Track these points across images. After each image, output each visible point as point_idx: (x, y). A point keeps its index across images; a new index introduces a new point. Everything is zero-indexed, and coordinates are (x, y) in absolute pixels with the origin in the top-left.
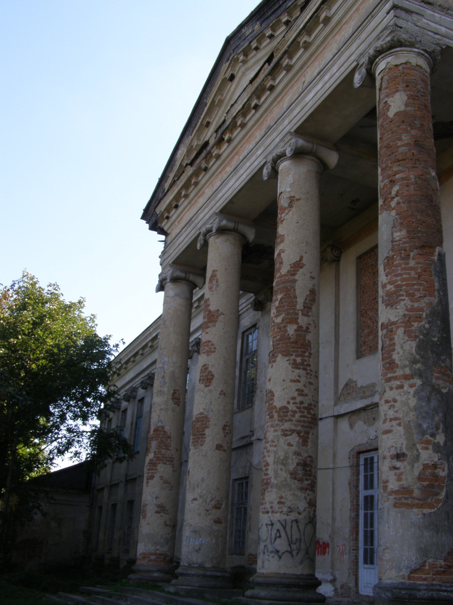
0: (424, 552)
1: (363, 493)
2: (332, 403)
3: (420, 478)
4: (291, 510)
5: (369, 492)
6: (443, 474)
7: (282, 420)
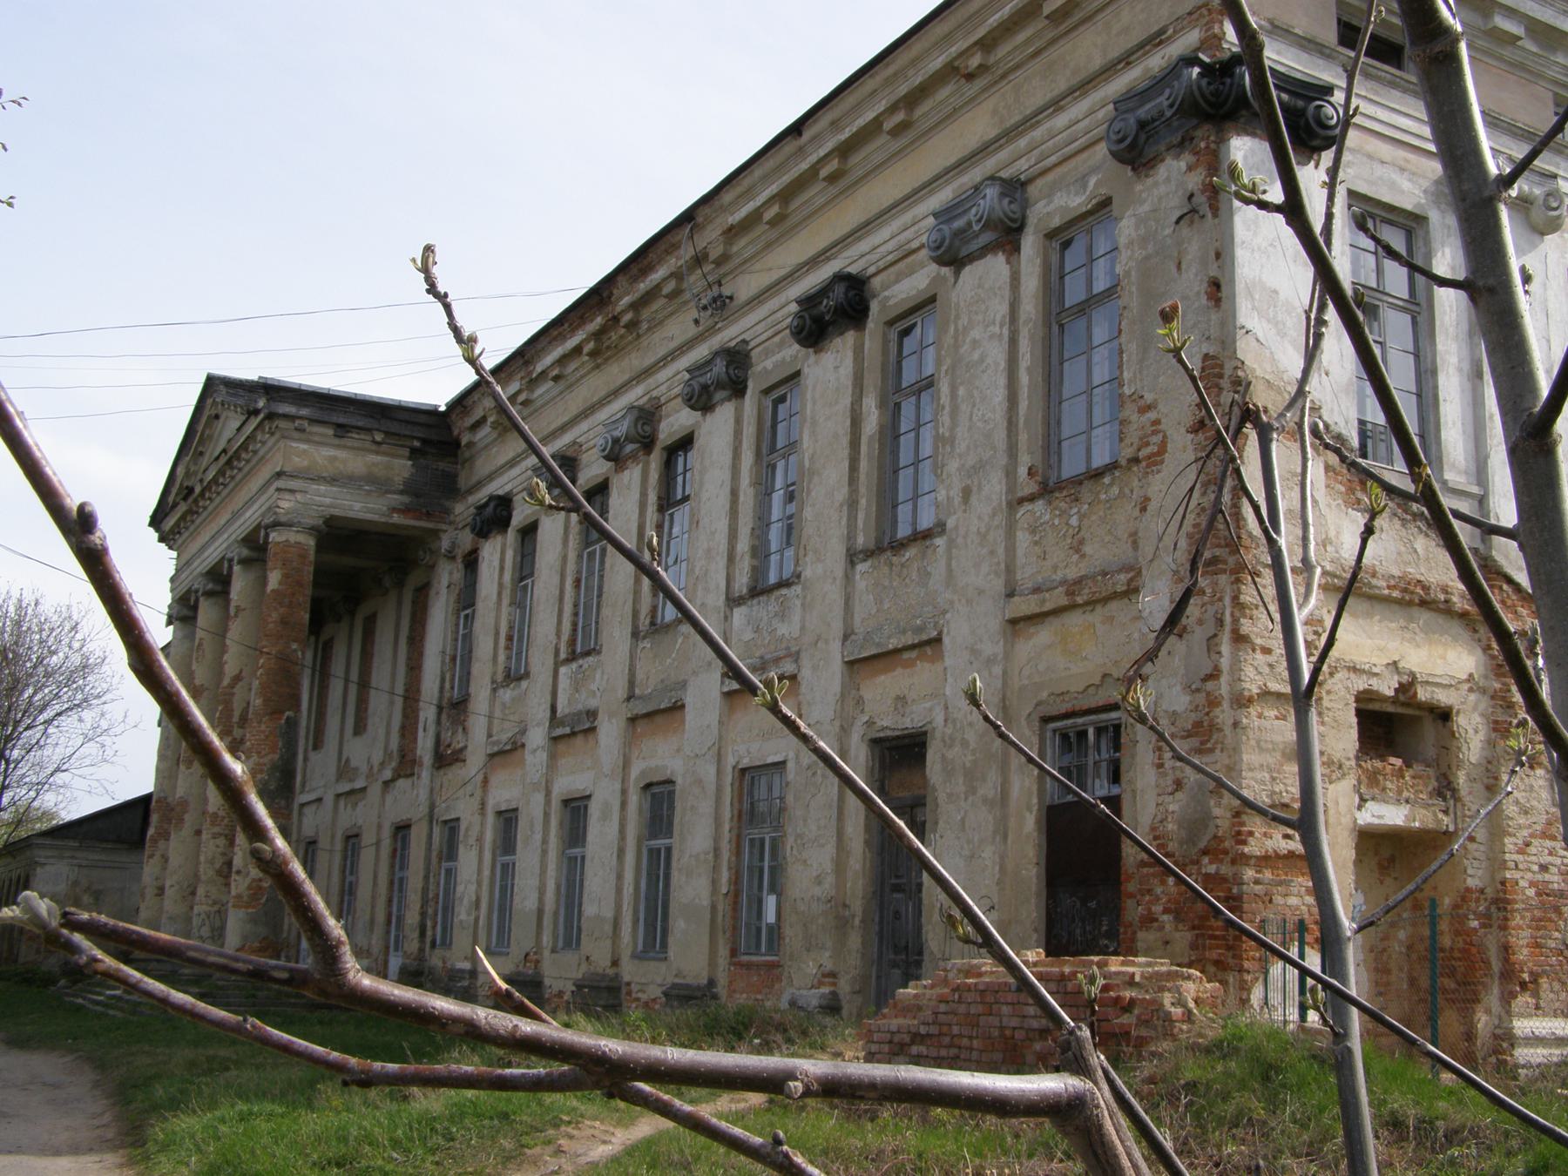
0: (245, 938)
1: (349, 878)
2: (333, 779)
3: (249, 888)
4: (215, 903)
5: (353, 878)
6: (265, 885)
7: (213, 824)
